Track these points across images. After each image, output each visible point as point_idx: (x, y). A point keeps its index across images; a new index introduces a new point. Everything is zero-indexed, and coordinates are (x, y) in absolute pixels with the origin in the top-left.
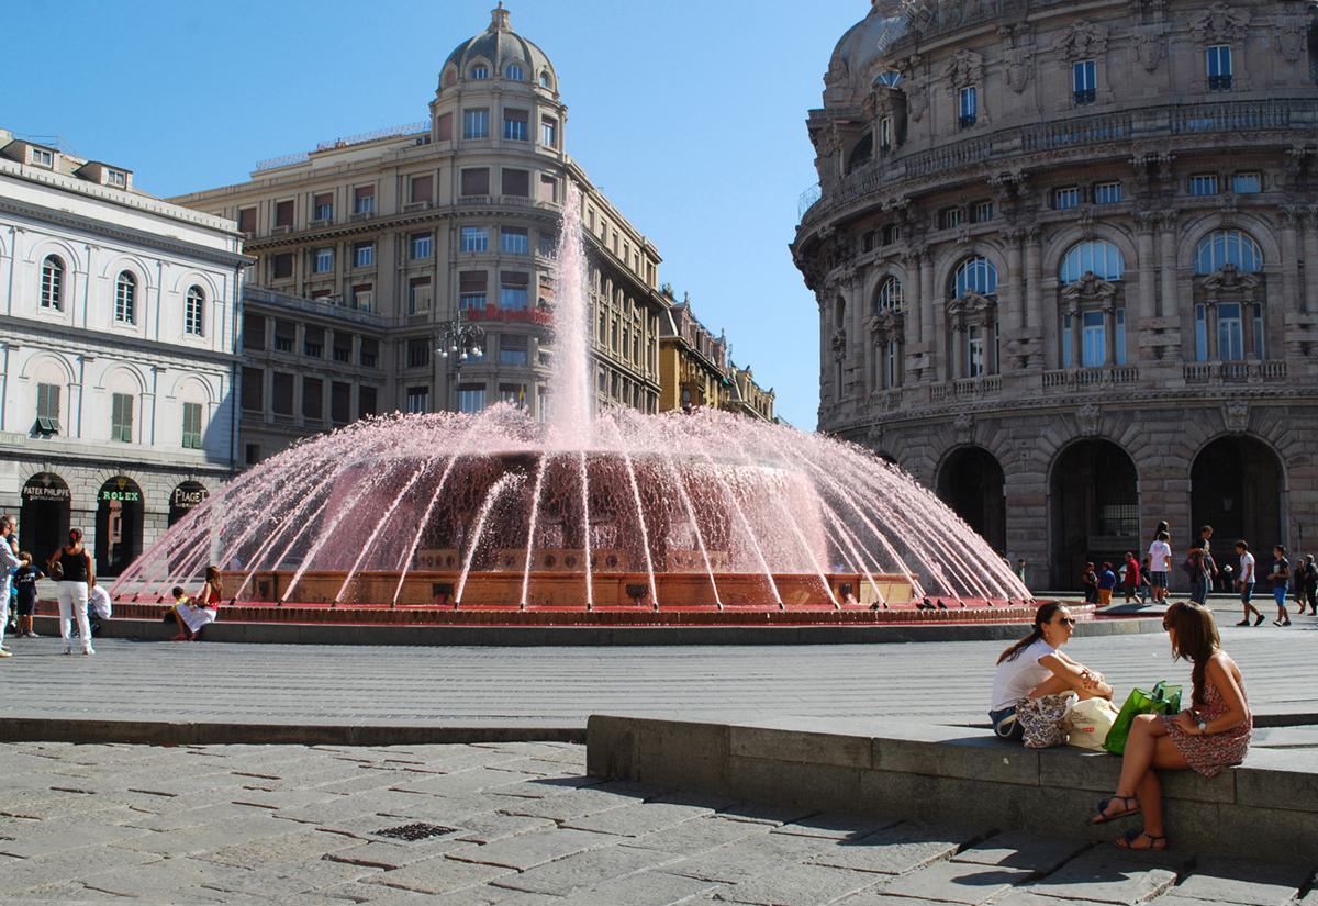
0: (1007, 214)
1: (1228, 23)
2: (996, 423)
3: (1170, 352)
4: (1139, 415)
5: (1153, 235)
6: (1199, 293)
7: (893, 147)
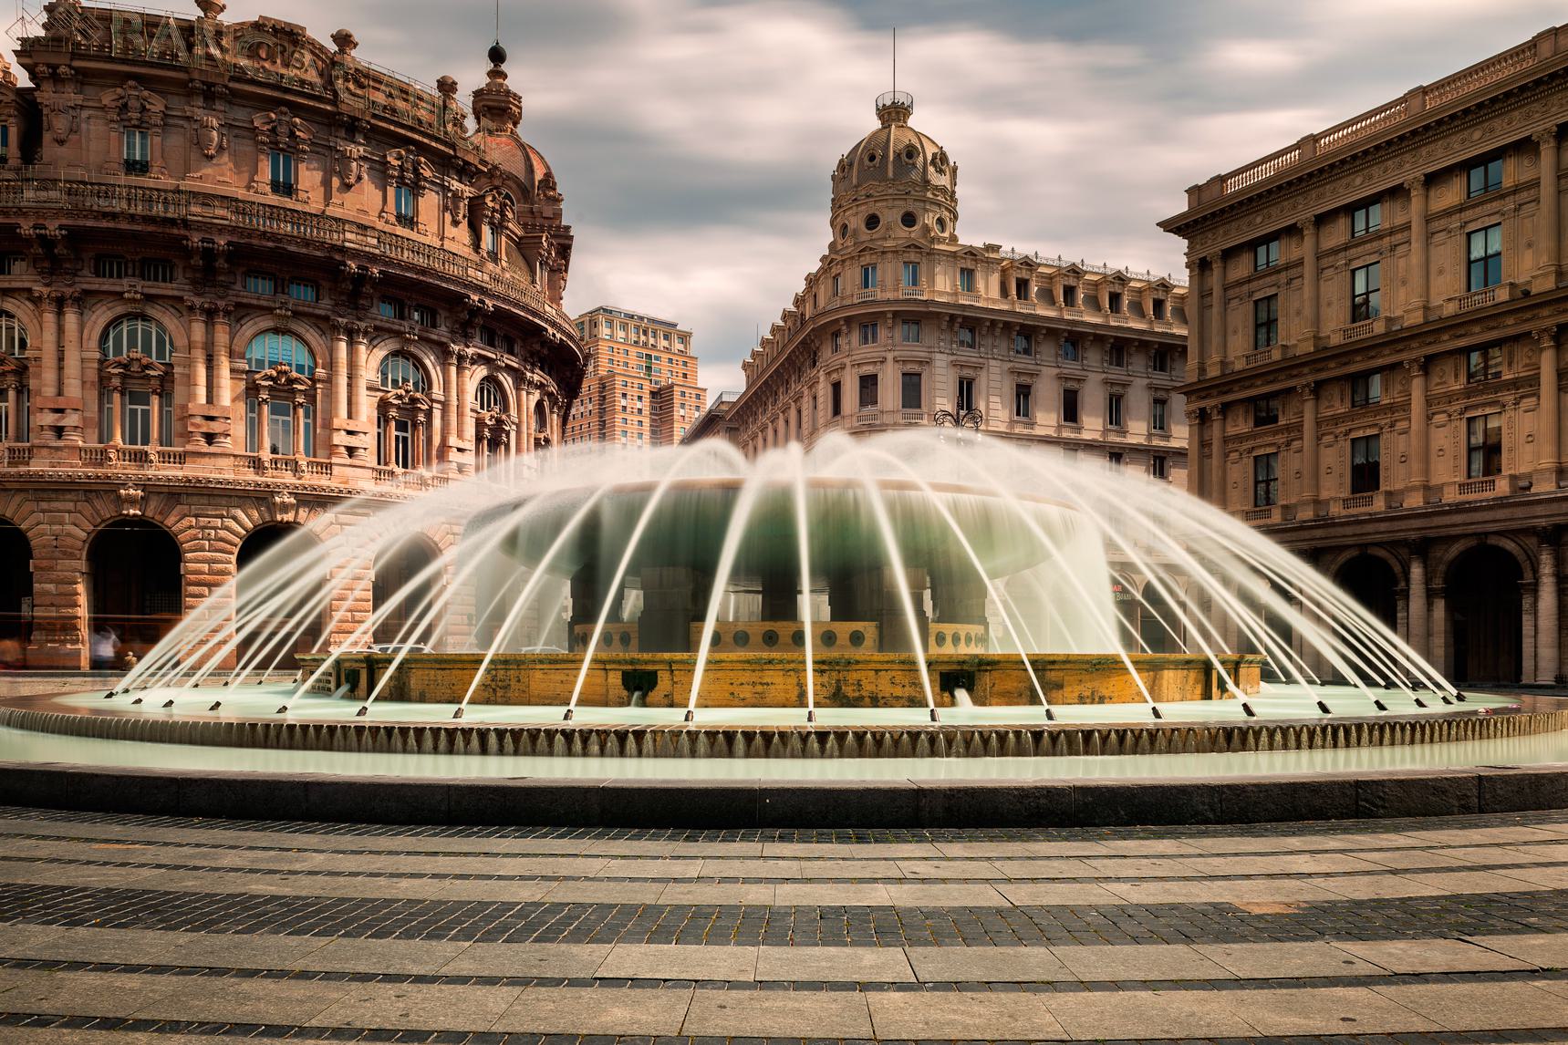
0: (194, 282)
6: (383, 406)
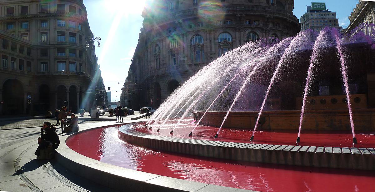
5: (239, 32)
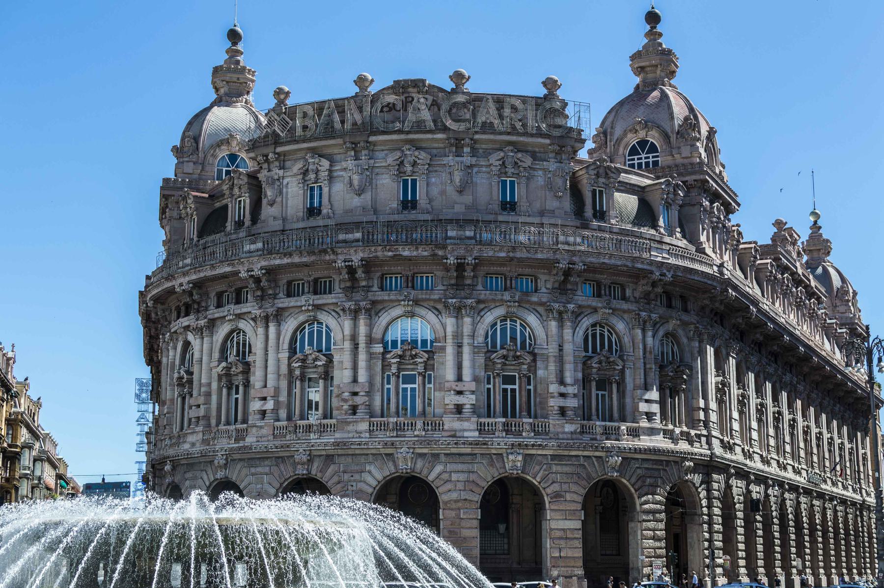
0: (345, 290)
1: (516, 163)
2: (329, 459)
3: (467, 409)
4: (443, 458)
5: (457, 317)
6: (489, 364)
7: (247, 222)
